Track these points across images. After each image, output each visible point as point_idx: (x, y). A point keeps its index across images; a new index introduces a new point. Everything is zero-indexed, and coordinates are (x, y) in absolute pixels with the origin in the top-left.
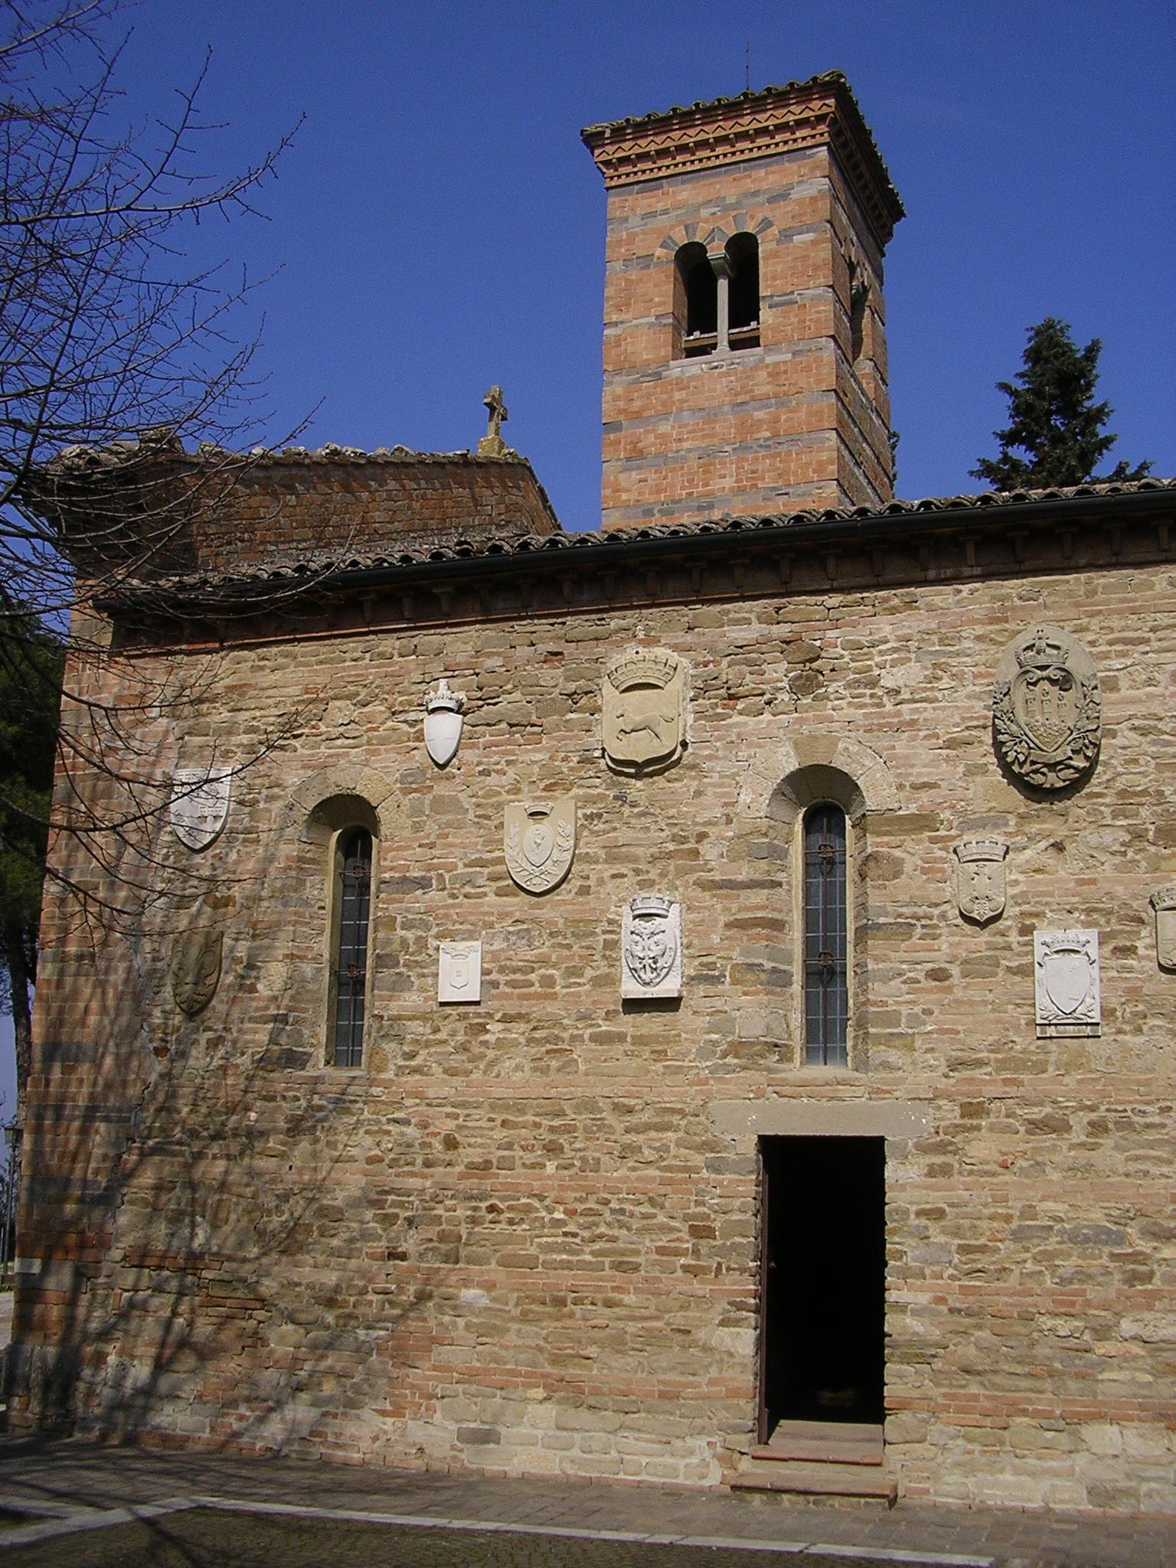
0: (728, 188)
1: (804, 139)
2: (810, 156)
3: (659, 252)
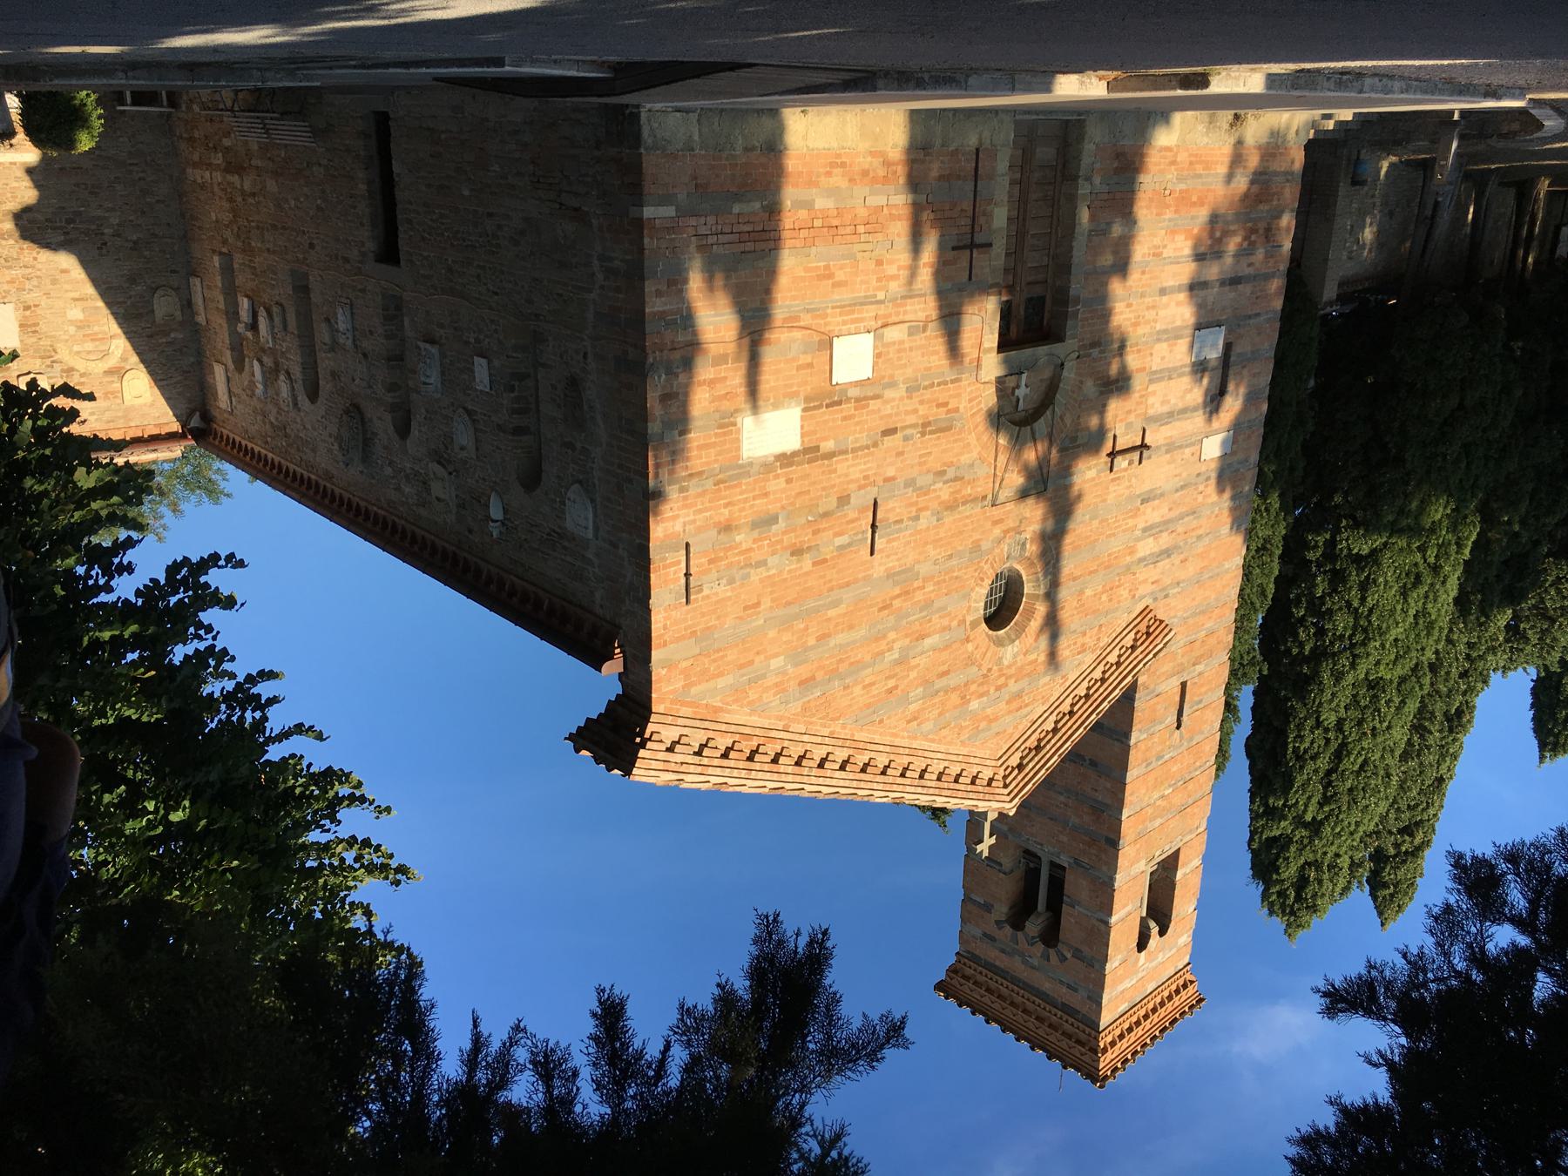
0: (1016, 966)
1: (970, 967)
2: (968, 952)
3: (1069, 956)
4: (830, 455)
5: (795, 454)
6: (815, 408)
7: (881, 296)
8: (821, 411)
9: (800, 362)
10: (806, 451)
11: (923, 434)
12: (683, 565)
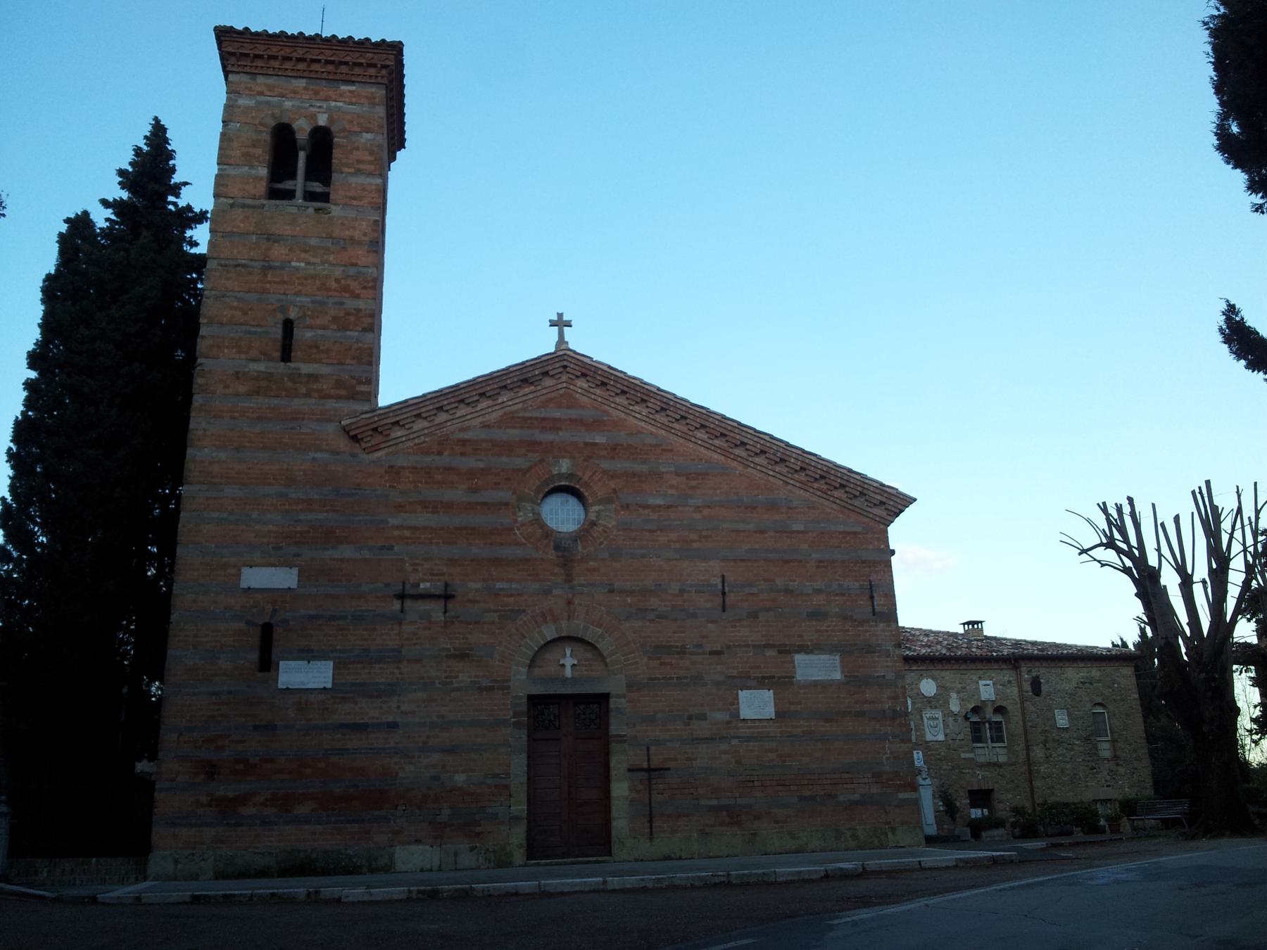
4: (767, 646)
5: (799, 652)
6: (786, 677)
7: (734, 742)
8: (779, 675)
9: (799, 706)
10: (790, 652)
11: (683, 647)
12: (875, 603)
